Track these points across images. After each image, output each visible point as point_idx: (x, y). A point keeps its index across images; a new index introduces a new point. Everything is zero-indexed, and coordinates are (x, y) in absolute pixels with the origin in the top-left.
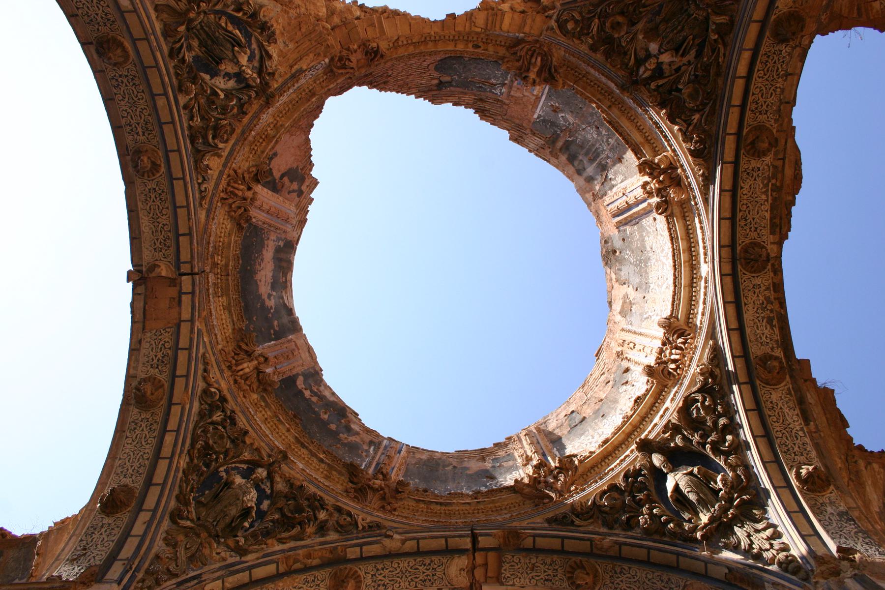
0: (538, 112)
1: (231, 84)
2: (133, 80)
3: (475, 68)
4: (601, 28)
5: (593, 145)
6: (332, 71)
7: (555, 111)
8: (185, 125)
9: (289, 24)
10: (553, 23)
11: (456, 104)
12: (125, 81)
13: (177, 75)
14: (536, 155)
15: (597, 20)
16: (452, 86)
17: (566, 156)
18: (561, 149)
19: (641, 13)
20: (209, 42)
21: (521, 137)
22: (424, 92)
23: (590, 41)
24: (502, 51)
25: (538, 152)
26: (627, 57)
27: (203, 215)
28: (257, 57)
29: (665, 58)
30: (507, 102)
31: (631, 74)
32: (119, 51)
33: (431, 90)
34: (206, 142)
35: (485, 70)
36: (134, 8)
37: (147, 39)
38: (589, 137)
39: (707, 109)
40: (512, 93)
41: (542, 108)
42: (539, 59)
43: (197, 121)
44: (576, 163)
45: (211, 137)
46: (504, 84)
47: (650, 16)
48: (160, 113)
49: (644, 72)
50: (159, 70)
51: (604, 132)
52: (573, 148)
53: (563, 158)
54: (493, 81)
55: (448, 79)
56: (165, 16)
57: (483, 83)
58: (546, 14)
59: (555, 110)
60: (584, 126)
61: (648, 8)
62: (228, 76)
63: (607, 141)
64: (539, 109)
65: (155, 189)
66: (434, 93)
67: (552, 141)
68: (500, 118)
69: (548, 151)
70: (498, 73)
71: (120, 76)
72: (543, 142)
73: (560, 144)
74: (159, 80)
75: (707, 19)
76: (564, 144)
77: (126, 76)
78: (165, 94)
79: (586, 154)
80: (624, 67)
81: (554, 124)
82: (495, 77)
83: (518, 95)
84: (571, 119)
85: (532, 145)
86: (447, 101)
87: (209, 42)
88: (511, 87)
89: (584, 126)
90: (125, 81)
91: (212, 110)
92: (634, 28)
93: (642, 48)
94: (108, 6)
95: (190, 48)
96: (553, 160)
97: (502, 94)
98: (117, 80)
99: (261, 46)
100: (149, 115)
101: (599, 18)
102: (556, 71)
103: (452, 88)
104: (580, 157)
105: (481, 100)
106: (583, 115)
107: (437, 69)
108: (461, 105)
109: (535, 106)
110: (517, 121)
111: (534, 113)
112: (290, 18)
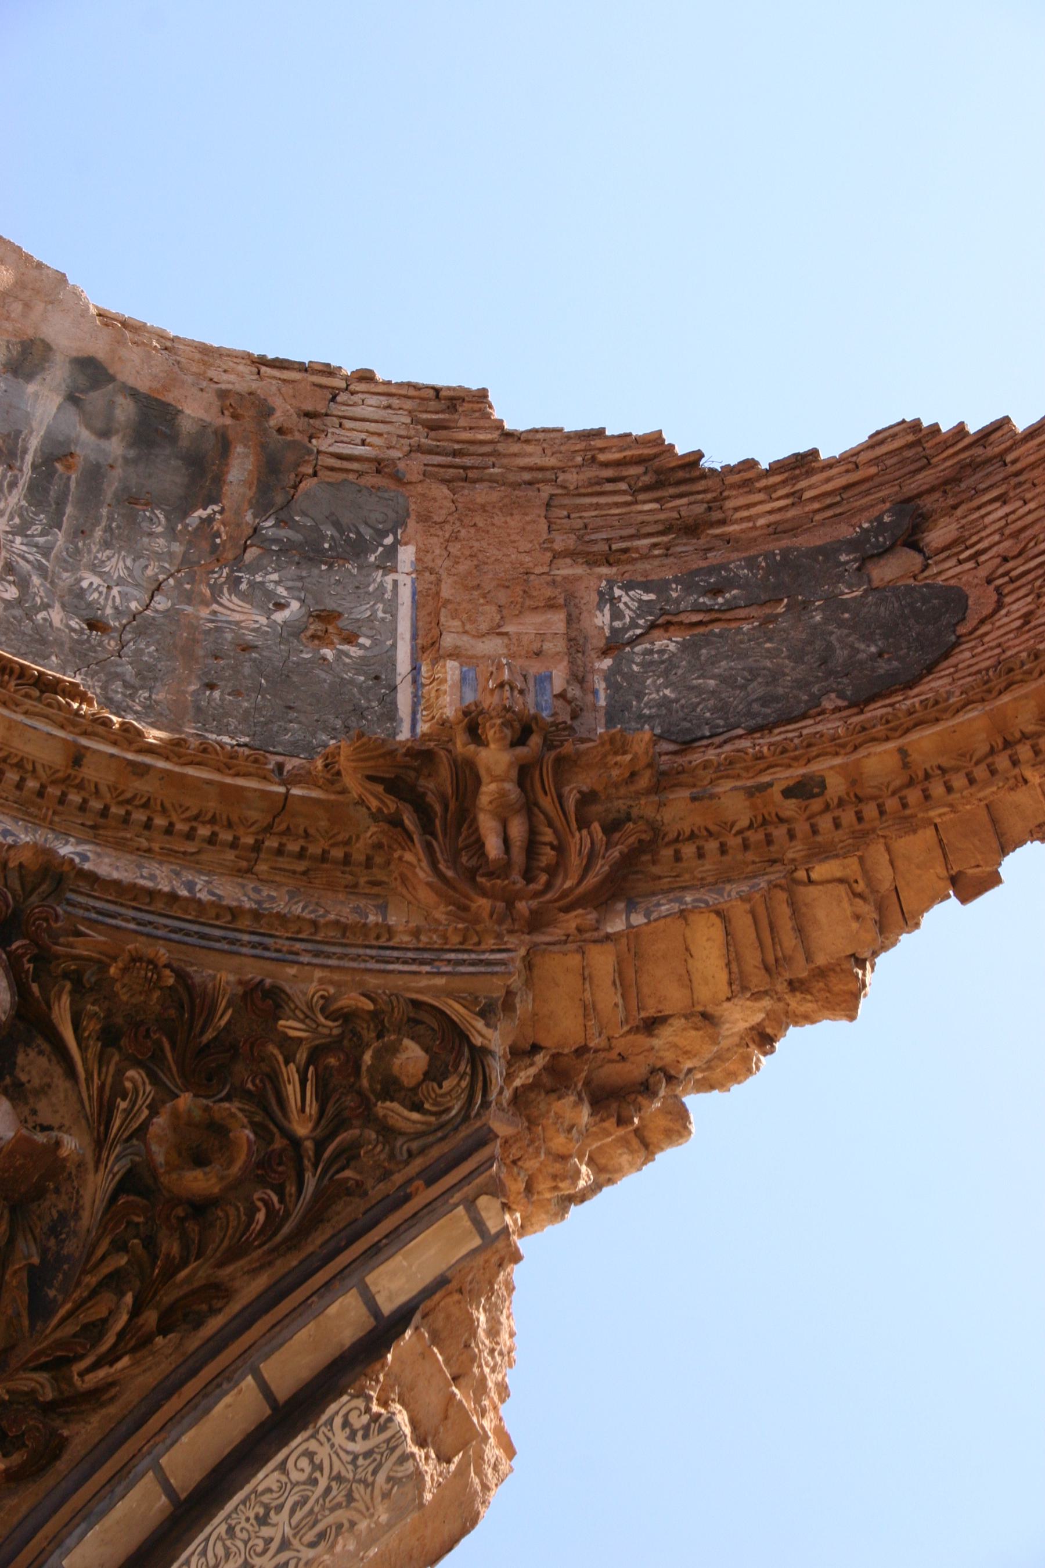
0: (403, 581)
3: (775, 676)
4: (266, 1104)
5: (81, 532)
7: (326, 617)
10: (494, 1038)
11: (803, 463)
14: (328, 371)
15: (302, 1129)
16: (853, 545)
17: (186, 426)
18: (225, 446)
19: (119, 1246)
21: (433, 427)
22: (974, 466)
23: (291, 1027)
24: (678, 812)
25: (326, 389)
26: (92, 1027)
30: (566, 569)
31: (43, 958)
33: (945, 485)
35: (726, 680)
38: (117, 565)
40: (557, 621)
41: (392, 607)
42: (493, 846)
44: (125, 410)
46: (613, 646)
47: (72, 1247)
51: (56, 616)
52: (168, 476)
53: (195, 409)
54: (667, 643)
55: (889, 571)
57: (715, 615)
58: (541, 1060)
59: (325, 622)
60: (161, 603)
61: (91, 1280)
63: (23, 584)
64: (405, 595)
66: (926, 478)
67: (280, 471)
68: (571, 478)
69: (283, 412)
70: (657, 690)
72: (323, 444)
73: (240, 470)
76: (219, 480)
79: (95, 474)
80: (89, 977)
81: (309, 553)
82: (667, 666)
83: (526, 627)
84: (239, 613)
85: (370, 407)
86: (850, 460)
88: (575, 645)
89: (161, 603)
92: (120, 1168)
93: (44, 1090)
96: (241, 381)
97: (606, 598)
101: (295, 1143)
102: (395, 822)
103: (846, 531)
104: (115, 447)
105: (691, 529)
106: (188, 653)
107: (955, 600)
108: (777, 467)
109: (428, 603)
110: (482, 494)
111: (421, 568)
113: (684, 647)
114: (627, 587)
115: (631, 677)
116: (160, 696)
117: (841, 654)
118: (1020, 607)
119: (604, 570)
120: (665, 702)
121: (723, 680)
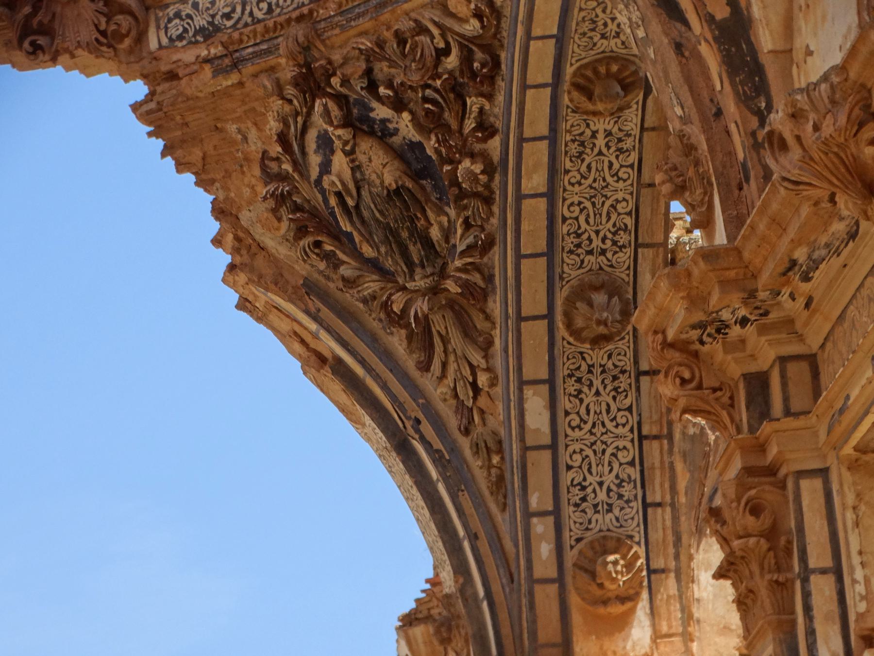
1: (381, 112)
2: (579, 246)
8: (500, 98)
9: (228, 174)
12: (597, 243)
13: (488, 201)
20: (405, 234)
28: (312, 137)
32: (579, 322)
34: (467, 58)
36: (521, 390)
37: (520, 319)
43: (474, 103)
45: (452, 61)
48: (545, 159)
56: (480, 323)
62: (382, 134)
65: (603, 36)
71: (603, 252)
74: (525, 226)
77: (590, 252)
78: (520, 198)
87: (405, 234)
90: (597, 243)
91: (434, 102)
94: (567, 413)
98: (615, 243)
99: (301, 166)
100: (567, 172)
112: (226, 188)
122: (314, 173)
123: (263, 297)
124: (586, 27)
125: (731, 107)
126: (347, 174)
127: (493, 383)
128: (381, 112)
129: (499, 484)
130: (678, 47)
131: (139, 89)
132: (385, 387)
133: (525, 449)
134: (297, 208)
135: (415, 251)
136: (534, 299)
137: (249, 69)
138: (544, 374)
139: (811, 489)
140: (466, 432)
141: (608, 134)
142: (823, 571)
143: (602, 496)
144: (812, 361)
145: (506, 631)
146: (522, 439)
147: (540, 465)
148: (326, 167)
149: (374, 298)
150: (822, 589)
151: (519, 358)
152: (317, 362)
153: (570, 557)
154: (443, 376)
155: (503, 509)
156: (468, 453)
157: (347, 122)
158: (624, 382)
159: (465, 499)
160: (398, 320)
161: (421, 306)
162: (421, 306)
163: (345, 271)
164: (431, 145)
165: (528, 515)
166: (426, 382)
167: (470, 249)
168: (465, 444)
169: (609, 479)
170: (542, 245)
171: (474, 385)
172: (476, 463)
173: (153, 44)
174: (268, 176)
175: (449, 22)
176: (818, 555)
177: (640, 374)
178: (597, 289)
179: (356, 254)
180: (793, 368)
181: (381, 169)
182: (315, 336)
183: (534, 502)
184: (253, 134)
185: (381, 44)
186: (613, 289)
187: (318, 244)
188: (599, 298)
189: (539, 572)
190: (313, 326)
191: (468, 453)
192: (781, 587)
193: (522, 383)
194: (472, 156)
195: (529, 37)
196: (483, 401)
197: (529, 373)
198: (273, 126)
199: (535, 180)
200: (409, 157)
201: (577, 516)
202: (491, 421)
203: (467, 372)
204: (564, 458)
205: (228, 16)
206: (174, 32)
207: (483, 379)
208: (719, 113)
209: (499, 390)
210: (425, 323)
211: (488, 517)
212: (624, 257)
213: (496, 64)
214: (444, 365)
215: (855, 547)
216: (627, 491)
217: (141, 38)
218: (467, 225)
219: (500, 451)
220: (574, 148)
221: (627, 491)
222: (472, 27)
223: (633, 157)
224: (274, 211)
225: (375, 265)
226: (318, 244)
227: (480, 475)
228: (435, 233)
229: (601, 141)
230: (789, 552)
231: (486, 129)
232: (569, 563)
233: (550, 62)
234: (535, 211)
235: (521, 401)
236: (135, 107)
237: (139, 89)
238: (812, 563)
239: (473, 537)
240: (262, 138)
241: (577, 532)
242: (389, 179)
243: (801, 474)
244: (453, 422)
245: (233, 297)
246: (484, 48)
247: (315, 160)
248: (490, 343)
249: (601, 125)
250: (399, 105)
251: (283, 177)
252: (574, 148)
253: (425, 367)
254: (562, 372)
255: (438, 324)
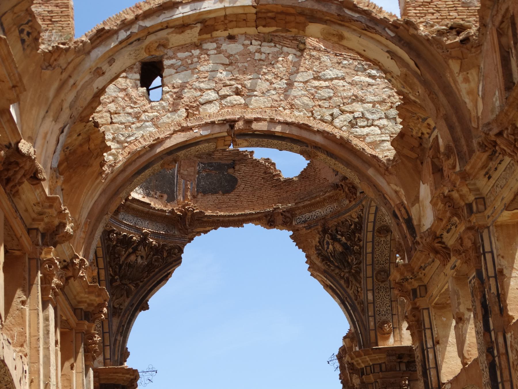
1: (339, 237)
6: (292, 215)
8: (362, 234)
9: (309, 249)
12: (382, 262)
13: (360, 254)
27: (364, 203)
28: (325, 241)
29: (133, 258)
32: (379, 278)
34: (356, 226)
37: (367, 277)
39: (111, 248)
40: (193, 168)
45: (353, 227)
46: (199, 173)
49: (141, 247)
50: (366, 263)
54: (204, 174)
56: (358, 278)
62: (339, 241)
66: (237, 158)
74: (367, 259)
75: (121, 281)
78: (366, 253)
95: (352, 261)
103: (226, 162)
113: (207, 175)
114: (201, 163)
115: (200, 179)
116: (152, 184)
117: (223, 183)
118: (243, 186)
119: (199, 159)
120: (203, 185)
121: (210, 183)
122: (326, 249)
123: (316, 273)
124: (379, 220)
125: (408, 236)
126: (332, 249)
127: (361, 290)
128: (339, 237)
129: (363, 310)
130: (398, 224)
131: (291, 233)
132: (340, 291)
133: (368, 303)
134: (322, 256)
135: (346, 264)
136: (369, 273)
137: (313, 229)
138: (372, 288)
139: (425, 313)
140: (356, 300)
141: (384, 241)
142: (428, 329)
143: (383, 313)
144: (426, 287)
145: (364, 340)
146: (367, 301)
147: (371, 307)
148: (328, 248)
149: (338, 273)
150: (428, 332)
151: (367, 285)
152: (327, 287)
153: (377, 325)
154: (351, 289)
155: (364, 315)
156: (356, 304)
157: (332, 239)
158: (387, 290)
159: (356, 315)
160: (342, 278)
161: (347, 275)
162: (347, 275)
163: (332, 268)
164: (349, 243)
165: (369, 316)
166: (348, 290)
167: (356, 264)
168: (356, 302)
169: (385, 309)
170: (371, 263)
171: (358, 291)
172: (358, 306)
173: (294, 224)
174: (317, 249)
175: (352, 219)
176: (427, 325)
177: (391, 288)
178: (382, 271)
179: (334, 265)
180: (421, 288)
181: (339, 248)
182: (326, 281)
183: (370, 314)
184: (313, 241)
185: (338, 223)
186: (385, 271)
187: (326, 263)
188: (383, 273)
189: (371, 328)
190: (326, 279)
191: (356, 304)
192: (420, 332)
193: (367, 290)
194: (357, 245)
195: (368, 222)
196: (359, 294)
197: (368, 288)
198: (317, 239)
199: (369, 250)
200: (344, 245)
201: (378, 317)
202: (361, 298)
203: (356, 288)
204: (376, 305)
205: (308, 218)
206: (298, 222)
207: (359, 289)
208: (406, 237)
209: (363, 291)
210: (348, 278)
211: (360, 317)
212: (387, 265)
213: (361, 227)
214: (352, 287)
215: (435, 324)
216: (388, 312)
217: (291, 223)
218: (356, 259)
219: (363, 304)
220: (377, 244)
221: (388, 312)
222: (357, 220)
223: (389, 245)
224: (318, 256)
225: (338, 267)
226: (326, 263)
227: (359, 309)
228: (350, 260)
229: (382, 242)
230: (421, 325)
231: (360, 240)
232: (377, 326)
233: (372, 227)
234: (369, 256)
235: (367, 294)
236: (290, 236)
237: (291, 233)
238: (426, 327)
239: (358, 321)
240: (315, 242)
241: (379, 320)
242: (340, 250)
243: (424, 309)
244: (353, 298)
245: (310, 273)
246: (359, 224)
247: (326, 246)
248: (361, 282)
249: (382, 239)
250: (342, 235)
251: (319, 250)
252: (377, 244)
253: (348, 287)
254: (375, 288)
255: (351, 278)
